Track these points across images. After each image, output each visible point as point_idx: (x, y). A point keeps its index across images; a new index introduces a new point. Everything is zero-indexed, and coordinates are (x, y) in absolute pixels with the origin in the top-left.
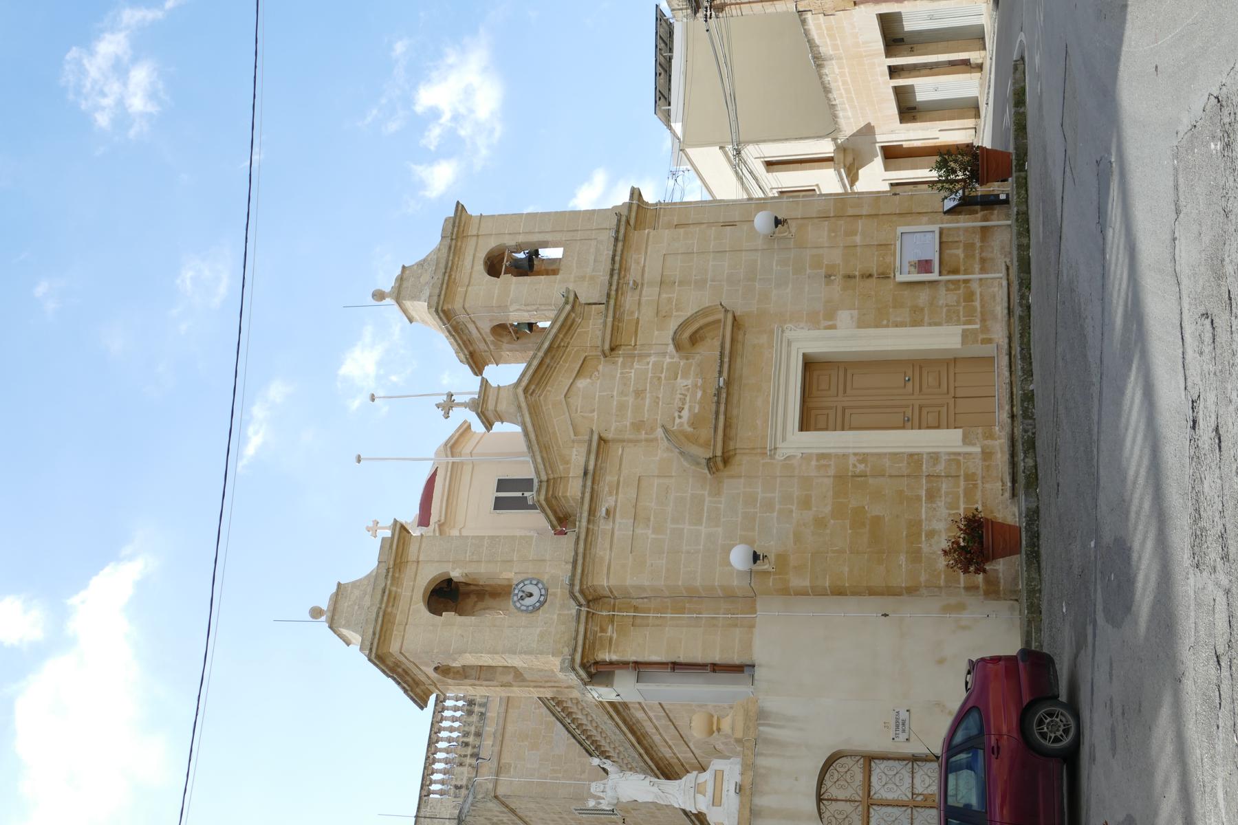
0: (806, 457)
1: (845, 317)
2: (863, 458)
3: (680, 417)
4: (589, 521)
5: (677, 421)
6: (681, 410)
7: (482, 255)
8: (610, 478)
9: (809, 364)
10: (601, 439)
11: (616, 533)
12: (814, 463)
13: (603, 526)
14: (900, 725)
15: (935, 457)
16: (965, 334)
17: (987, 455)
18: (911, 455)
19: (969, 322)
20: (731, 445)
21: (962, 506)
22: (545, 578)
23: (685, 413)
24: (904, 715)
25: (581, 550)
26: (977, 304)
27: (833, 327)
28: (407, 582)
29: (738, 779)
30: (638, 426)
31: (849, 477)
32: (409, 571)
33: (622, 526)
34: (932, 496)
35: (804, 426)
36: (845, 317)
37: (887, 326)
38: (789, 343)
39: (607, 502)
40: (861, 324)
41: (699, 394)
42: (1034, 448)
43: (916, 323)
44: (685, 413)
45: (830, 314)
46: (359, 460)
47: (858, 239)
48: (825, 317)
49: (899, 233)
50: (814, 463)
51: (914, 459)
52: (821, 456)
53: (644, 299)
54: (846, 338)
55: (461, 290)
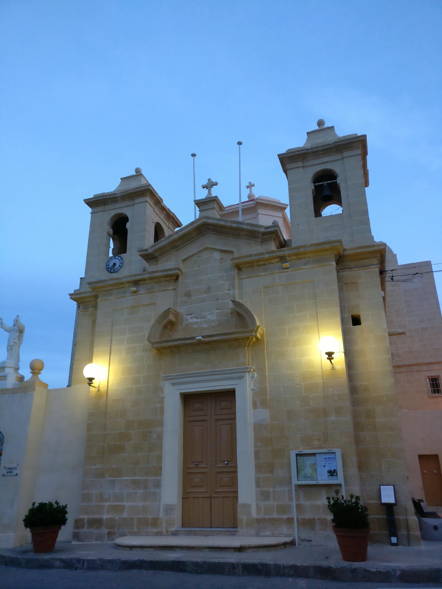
1: (264, 414)
2: (160, 437)
3: (192, 318)
5: (189, 317)
7: (328, 166)
12: (159, 405)
15: (158, 485)
16: (247, 507)
18: (161, 469)
19: (258, 509)
21: (126, 504)
22: (122, 270)
23: (195, 320)
24: (15, 472)
26: (275, 516)
30: (188, 294)
34: (135, 483)
37: (256, 446)
39: (142, 290)
40: (258, 427)
41: (205, 326)
43: (259, 468)
44: (195, 320)
45: (264, 404)
46: (194, 155)
47: (333, 418)
49: (334, 450)
52: (162, 410)
55: (300, 164)
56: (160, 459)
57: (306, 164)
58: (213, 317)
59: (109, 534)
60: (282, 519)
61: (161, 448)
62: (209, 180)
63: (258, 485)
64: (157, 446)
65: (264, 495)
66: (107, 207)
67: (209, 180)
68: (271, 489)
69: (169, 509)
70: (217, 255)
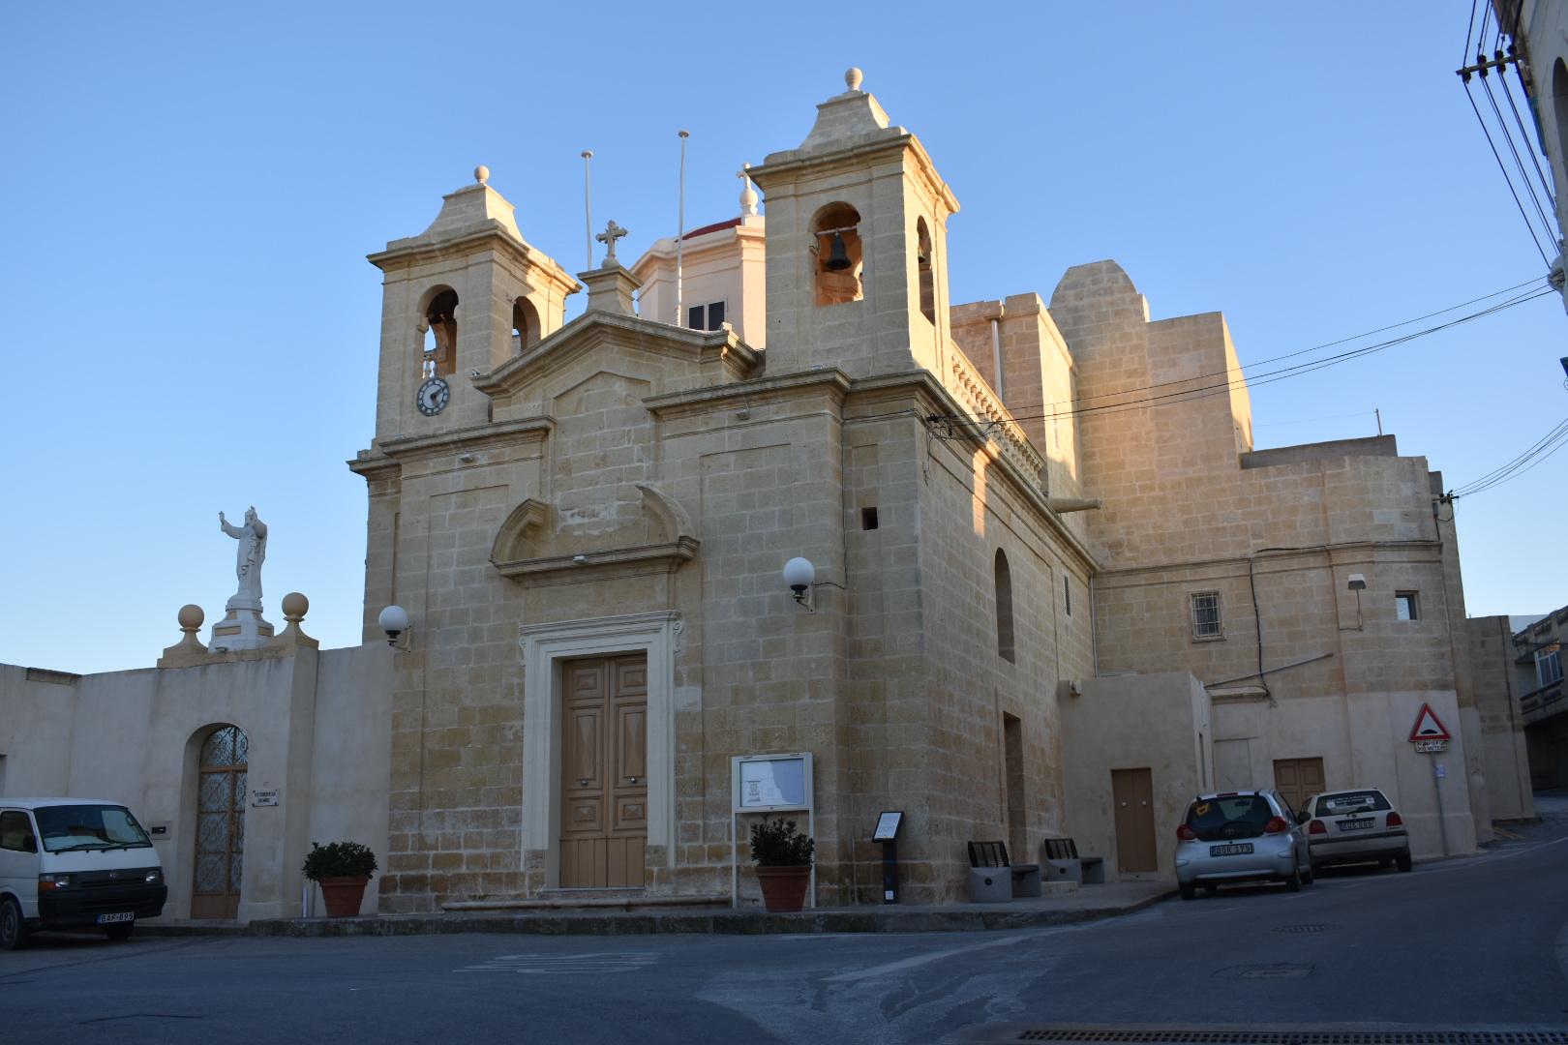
0: (521, 672)
2: (518, 738)
4: (454, 442)
6: (582, 515)
7: (843, 197)
8: (507, 452)
9: (640, 656)
10: (547, 430)
11: (450, 476)
12: (516, 680)
13: (457, 457)
14: (265, 797)
15: (516, 819)
17: (513, 879)
19: (680, 854)
20: (529, 583)
21: (465, 852)
23: (578, 520)
24: (273, 800)
25: (420, 444)
26: (706, 864)
27: (678, 681)
28: (438, 266)
29: (231, 649)
30: (567, 468)
31: (500, 724)
32: (457, 262)
33: (459, 479)
34: (479, 817)
35: (566, 666)
36: (690, 696)
37: (678, 750)
38: (656, 630)
39: (482, 456)
40: (681, 718)
41: (596, 532)
42: (364, 933)
43: (680, 787)
44: (578, 520)
47: (806, 700)
48: (693, 668)
50: (516, 680)
51: (515, 796)
52: (521, 688)
53: (726, 433)
54: (664, 696)
55: (790, 189)
56: (518, 773)
57: (804, 188)
58: (610, 512)
59: (438, 900)
60: (712, 870)
61: (520, 756)
62: (611, 223)
63: (679, 815)
64: (512, 754)
65: (689, 832)
66: (415, 271)
67: (611, 223)
68: (700, 822)
69: (536, 856)
70: (620, 388)
